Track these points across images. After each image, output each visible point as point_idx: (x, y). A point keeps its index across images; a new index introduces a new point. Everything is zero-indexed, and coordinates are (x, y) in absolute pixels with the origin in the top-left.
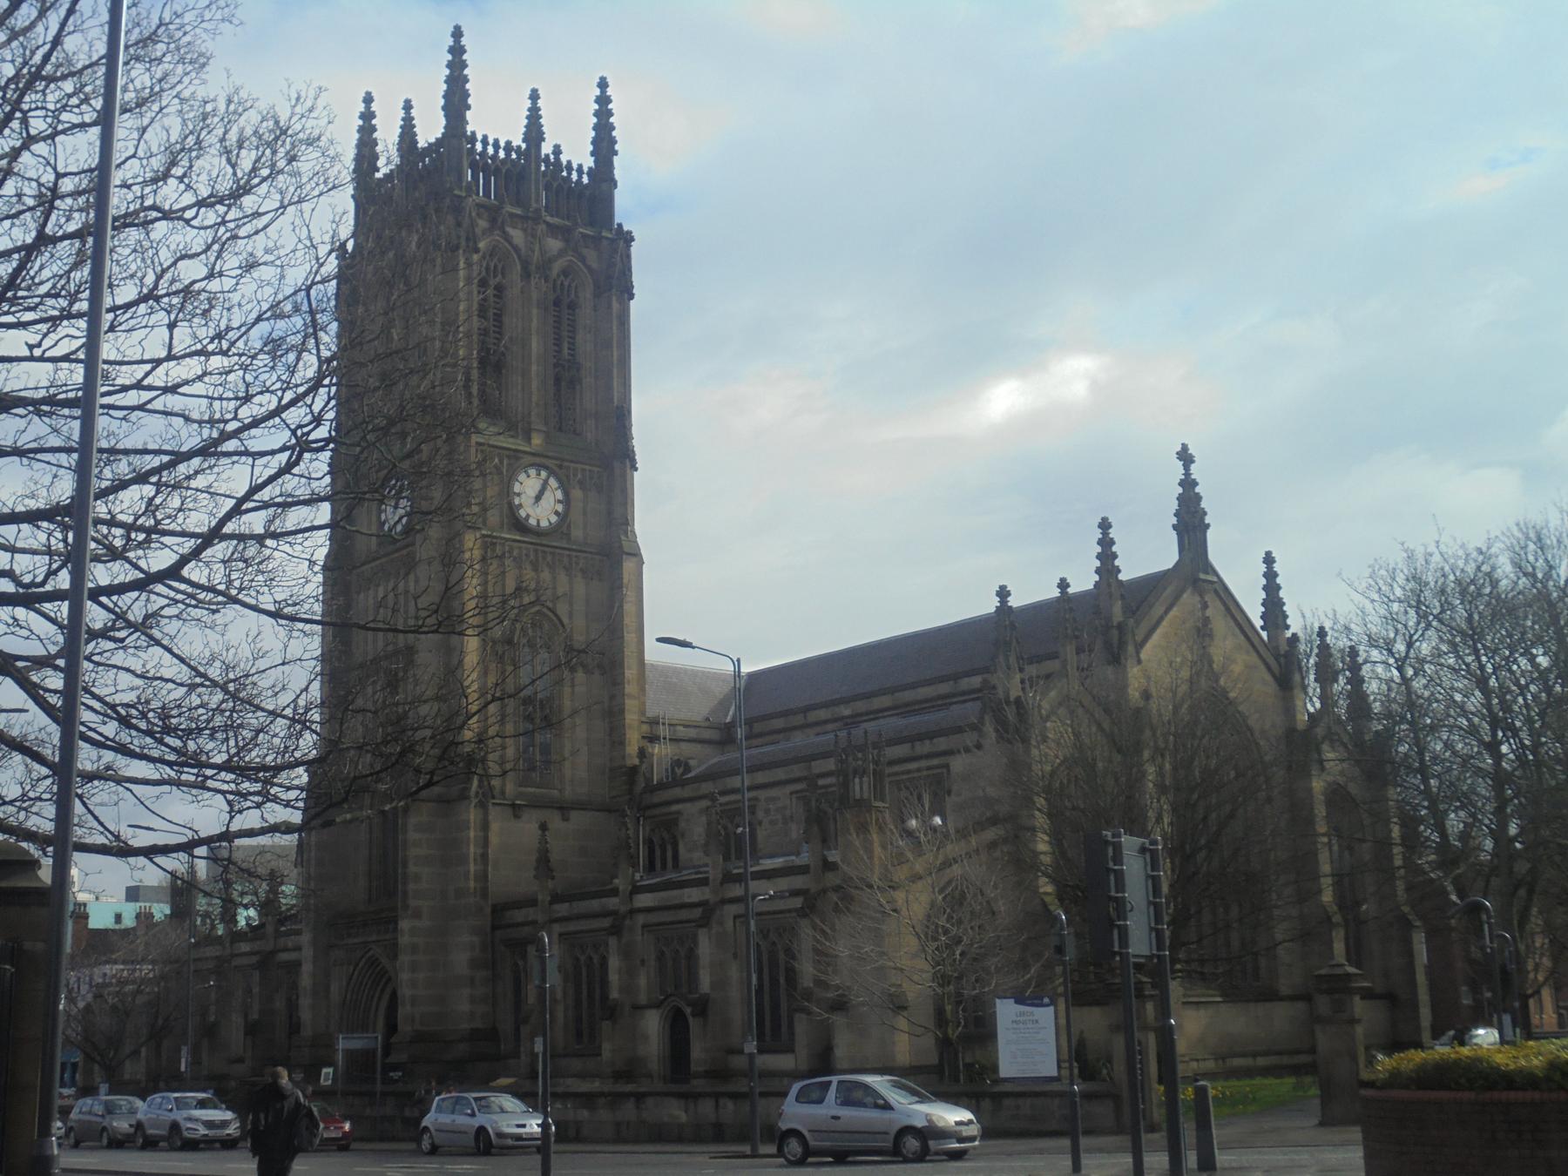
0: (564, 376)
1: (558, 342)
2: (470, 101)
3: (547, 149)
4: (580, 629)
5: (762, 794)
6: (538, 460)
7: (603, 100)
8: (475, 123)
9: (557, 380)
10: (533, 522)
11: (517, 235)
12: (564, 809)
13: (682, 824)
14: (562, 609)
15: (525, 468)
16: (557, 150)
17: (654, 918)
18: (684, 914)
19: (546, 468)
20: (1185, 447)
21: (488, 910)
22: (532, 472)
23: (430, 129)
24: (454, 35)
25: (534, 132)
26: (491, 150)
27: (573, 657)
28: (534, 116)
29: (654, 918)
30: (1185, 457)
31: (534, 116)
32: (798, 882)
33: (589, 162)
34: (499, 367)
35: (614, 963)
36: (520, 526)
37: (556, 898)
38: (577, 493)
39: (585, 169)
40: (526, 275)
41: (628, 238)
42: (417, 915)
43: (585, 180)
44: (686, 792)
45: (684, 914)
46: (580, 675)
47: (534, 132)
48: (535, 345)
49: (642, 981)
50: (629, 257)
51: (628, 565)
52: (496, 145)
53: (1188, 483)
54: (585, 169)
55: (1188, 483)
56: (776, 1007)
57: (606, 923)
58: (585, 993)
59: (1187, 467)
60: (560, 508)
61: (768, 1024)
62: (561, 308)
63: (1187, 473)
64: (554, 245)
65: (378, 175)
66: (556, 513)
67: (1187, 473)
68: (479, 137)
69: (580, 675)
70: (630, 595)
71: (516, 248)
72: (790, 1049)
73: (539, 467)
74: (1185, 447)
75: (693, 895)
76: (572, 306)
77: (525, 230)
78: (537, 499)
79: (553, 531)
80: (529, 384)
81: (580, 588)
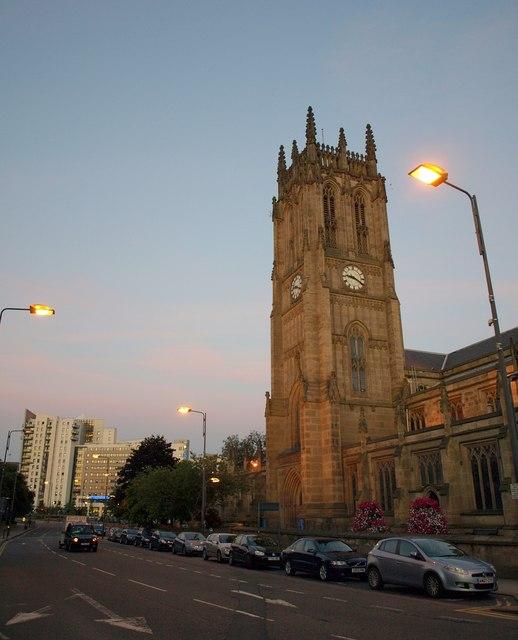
0: (362, 231)
1: (357, 220)
4: (378, 333)
5: (463, 392)
10: (352, 287)
11: (339, 180)
12: (373, 407)
13: (426, 410)
14: (367, 322)
17: (415, 447)
18: (432, 444)
21: (340, 450)
27: (373, 342)
28: (342, 136)
29: (415, 447)
31: (342, 136)
32: (495, 421)
33: (365, 154)
34: (333, 229)
35: (399, 470)
36: (346, 290)
37: (369, 441)
41: (384, 179)
42: (308, 452)
44: (427, 395)
45: (432, 444)
49: (413, 479)
51: (393, 304)
56: (487, 490)
57: (393, 451)
58: (385, 485)
61: (483, 496)
62: (359, 208)
64: (354, 183)
70: (397, 333)
71: (339, 184)
72: (500, 512)
73: (353, 266)
75: (436, 433)
76: (363, 207)
78: (353, 277)
80: (346, 236)
81: (374, 314)
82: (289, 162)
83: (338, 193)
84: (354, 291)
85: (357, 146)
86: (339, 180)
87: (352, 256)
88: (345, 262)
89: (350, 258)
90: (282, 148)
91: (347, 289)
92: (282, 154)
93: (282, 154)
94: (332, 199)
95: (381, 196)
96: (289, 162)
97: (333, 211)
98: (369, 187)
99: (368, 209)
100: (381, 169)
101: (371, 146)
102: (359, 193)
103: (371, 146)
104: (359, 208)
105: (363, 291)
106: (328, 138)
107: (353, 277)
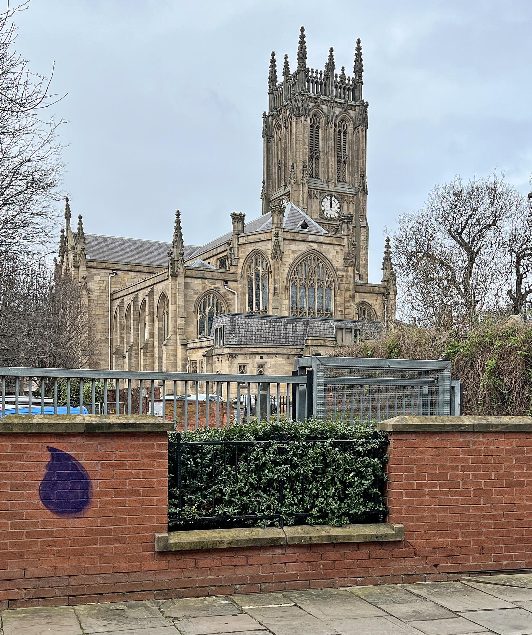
2: (307, 56)
3: (337, 71)
7: (359, 49)
8: (310, 64)
9: (339, 162)
16: (343, 70)
23: (294, 67)
24: (301, 31)
25: (330, 66)
26: (314, 75)
33: (352, 75)
39: (351, 79)
41: (367, 105)
43: (351, 82)
47: (330, 66)
50: (366, 112)
52: (317, 73)
64: (338, 111)
65: (277, 84)
66: (337, 212)
68: (310, 70)
77: (328, 105)
82: (280, 79)
83: (323, 122)
85: (345, 65)
90: (273, 55)
92: (273, 61)
93: (273, 61)
94: (318, 128)
95: (363, 122)
96: (280, 79)
98: (352, 113)
99: (349, 137)
100: (365, 97)
101: (359, 69)
102: (343, 120)
103: (359, 69)
104: (342, 133)
106: (316, 63)
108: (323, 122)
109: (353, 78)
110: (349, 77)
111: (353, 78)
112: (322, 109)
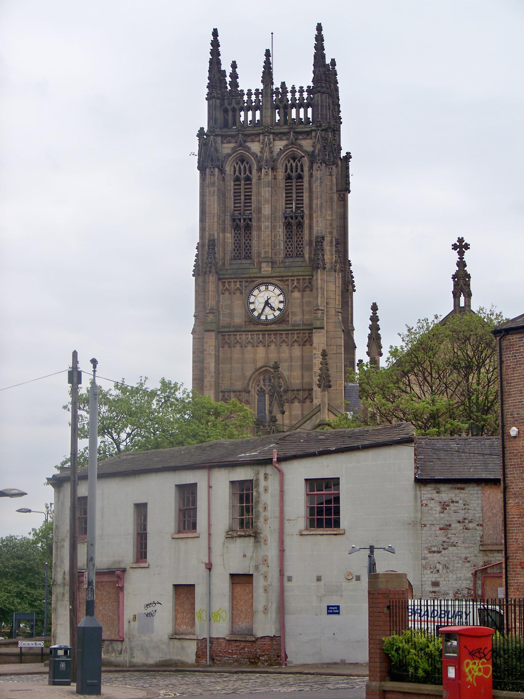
6: (265, 280)
15: (257, 287)
19: (272, 284)
20: (461, 240)
22: (263, 288)
30: (461, 247)
34: (248, 228)
38: (297, 294)
39: (305, 88)
40: (260, 170)
46: (296, 404)
48: (266, 210)
53: (461, 264)
54: (305, 88)
55: (461, 264)
59: (461, 254)
60: (281, 306)
63: (461, 258)
67: (461, 258)
69: (296, 404)
71: (253, 154)
73: (267, 284)
74: (461, 240)
76: (300, 177)
79: (278, 321)
80: (268, 234)
83: (255, 167)
84: (267, 322)
86: (255, 147)
87: (266, 269)
88: (254, 282)
89: (263, 273)
91: (257, 321)
94: (248, 179)
97: (248, 197)
105: (281, 320)
107: (267, 300)
108: (255, 167)
109: (309, 87)
110: (293, 87)
111: (309, 87)
112: (248, 149)
